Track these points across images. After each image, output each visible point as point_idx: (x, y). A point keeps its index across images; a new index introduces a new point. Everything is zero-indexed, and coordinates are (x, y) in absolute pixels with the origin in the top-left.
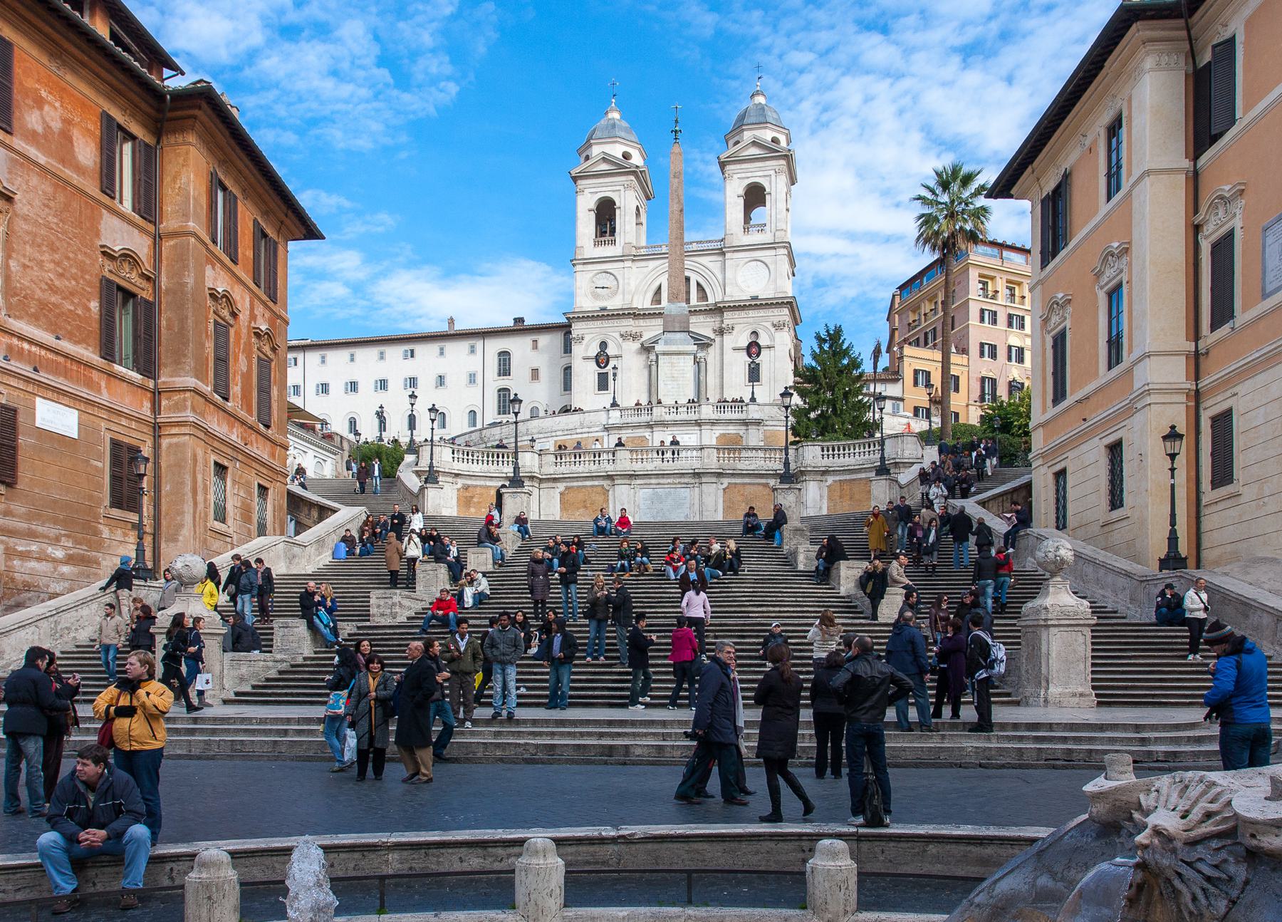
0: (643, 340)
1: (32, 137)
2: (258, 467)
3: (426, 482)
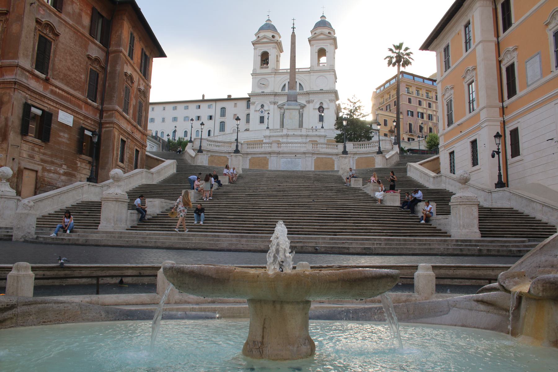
0: (278, 104)
1: (68, 14)
3: (198, 152)
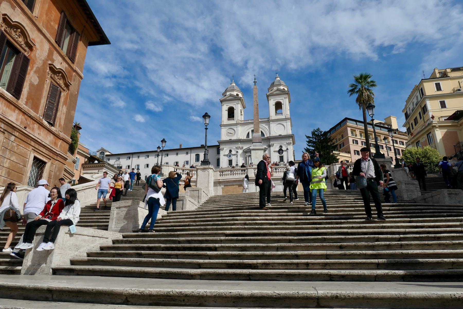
0: (243, 149)
2: (37, 146)
